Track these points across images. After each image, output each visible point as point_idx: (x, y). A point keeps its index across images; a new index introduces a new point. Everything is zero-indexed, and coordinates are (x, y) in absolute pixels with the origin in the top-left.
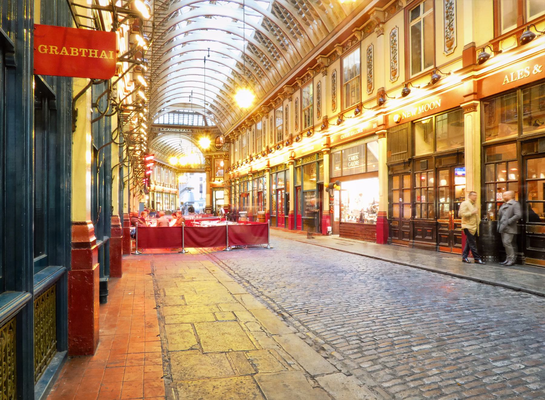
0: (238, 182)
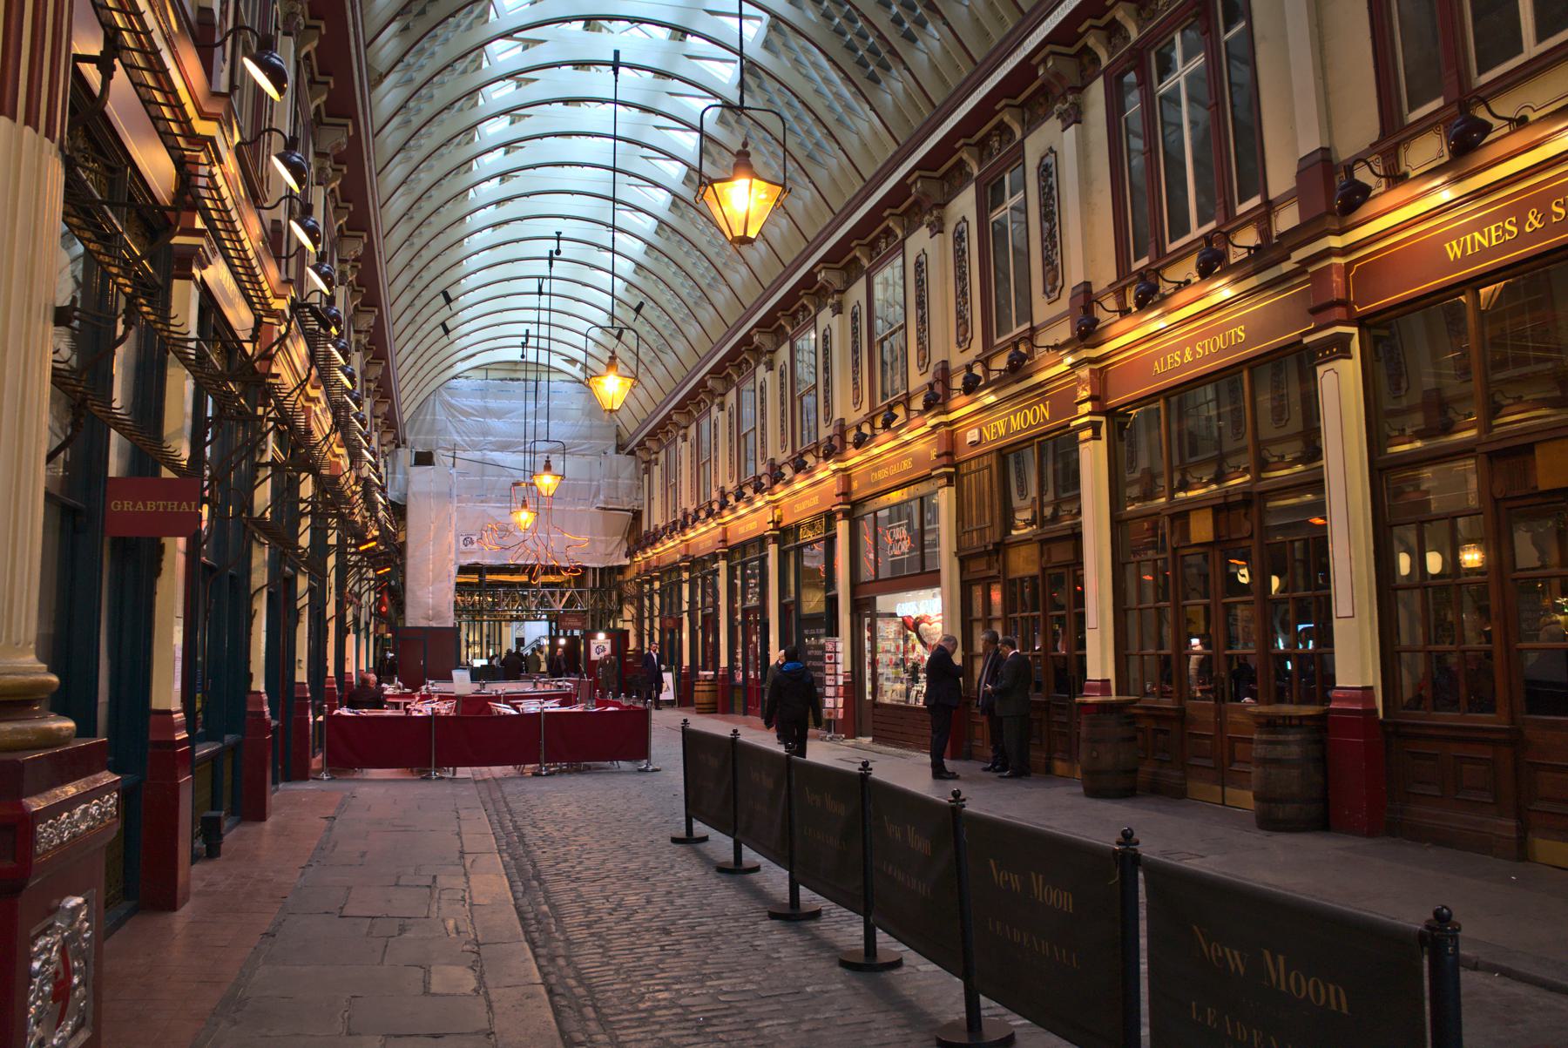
0: (657, 585)
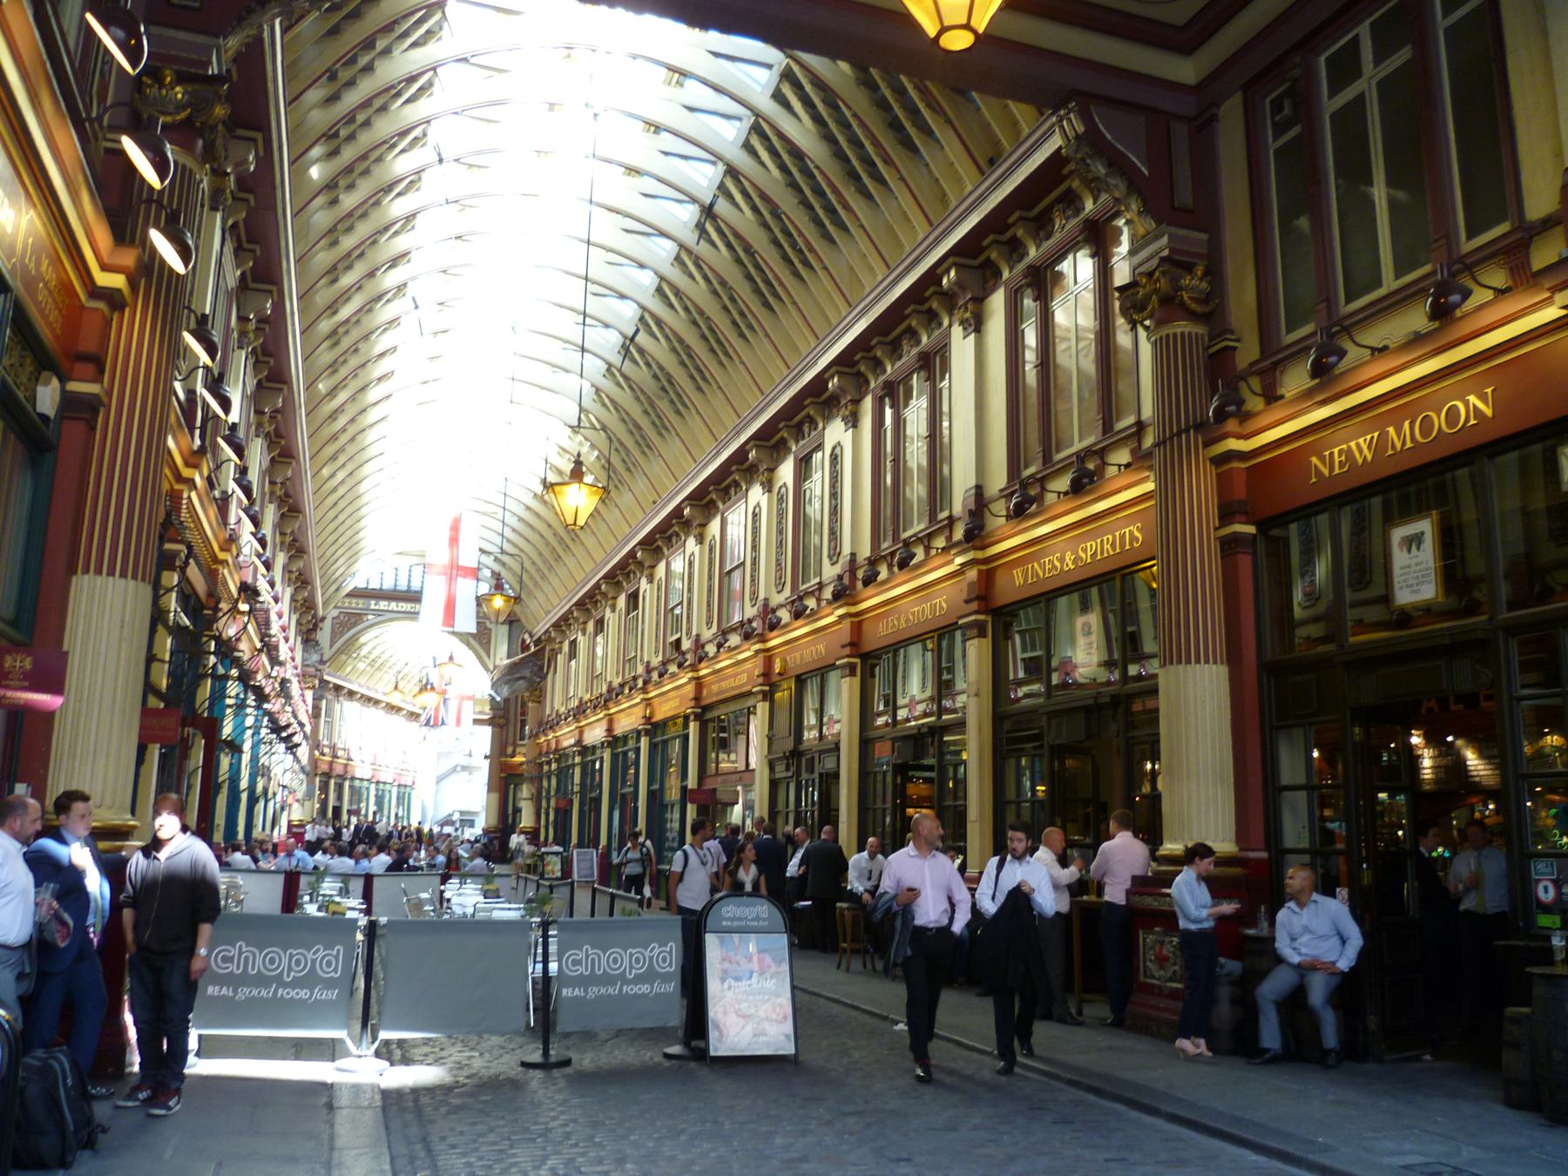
0: (554, 766)
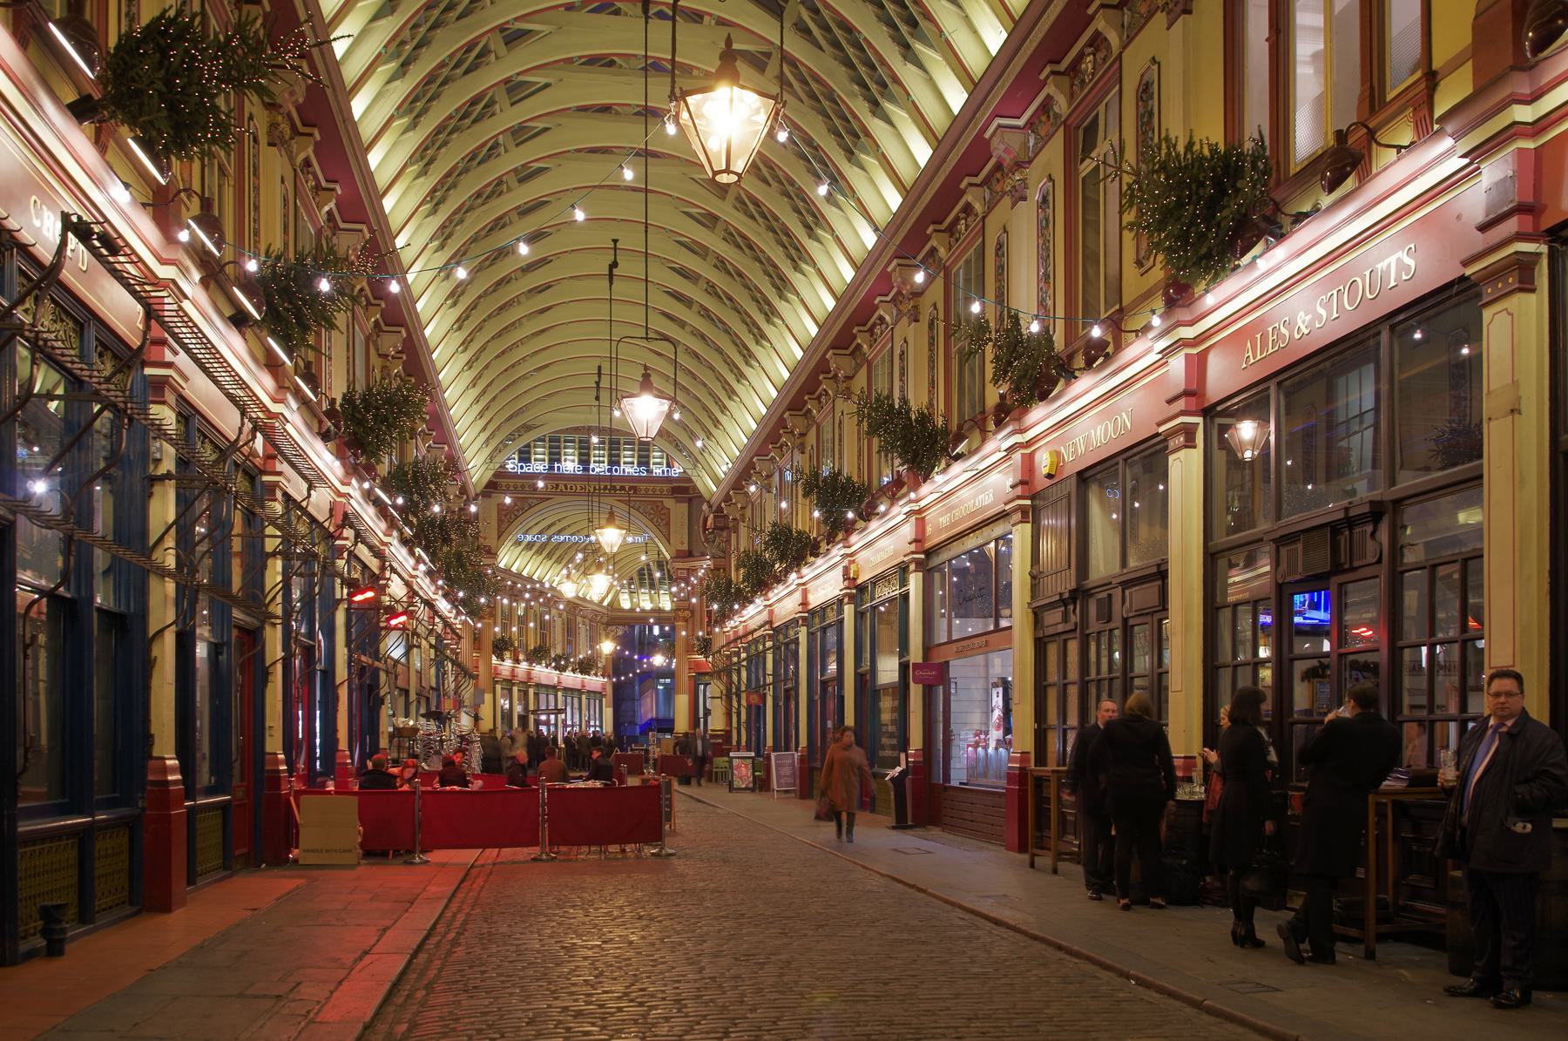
0: (744, 655)
